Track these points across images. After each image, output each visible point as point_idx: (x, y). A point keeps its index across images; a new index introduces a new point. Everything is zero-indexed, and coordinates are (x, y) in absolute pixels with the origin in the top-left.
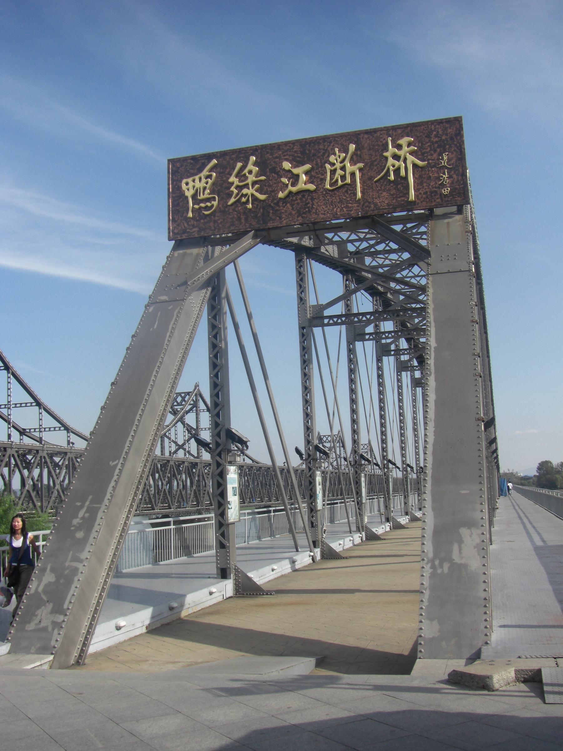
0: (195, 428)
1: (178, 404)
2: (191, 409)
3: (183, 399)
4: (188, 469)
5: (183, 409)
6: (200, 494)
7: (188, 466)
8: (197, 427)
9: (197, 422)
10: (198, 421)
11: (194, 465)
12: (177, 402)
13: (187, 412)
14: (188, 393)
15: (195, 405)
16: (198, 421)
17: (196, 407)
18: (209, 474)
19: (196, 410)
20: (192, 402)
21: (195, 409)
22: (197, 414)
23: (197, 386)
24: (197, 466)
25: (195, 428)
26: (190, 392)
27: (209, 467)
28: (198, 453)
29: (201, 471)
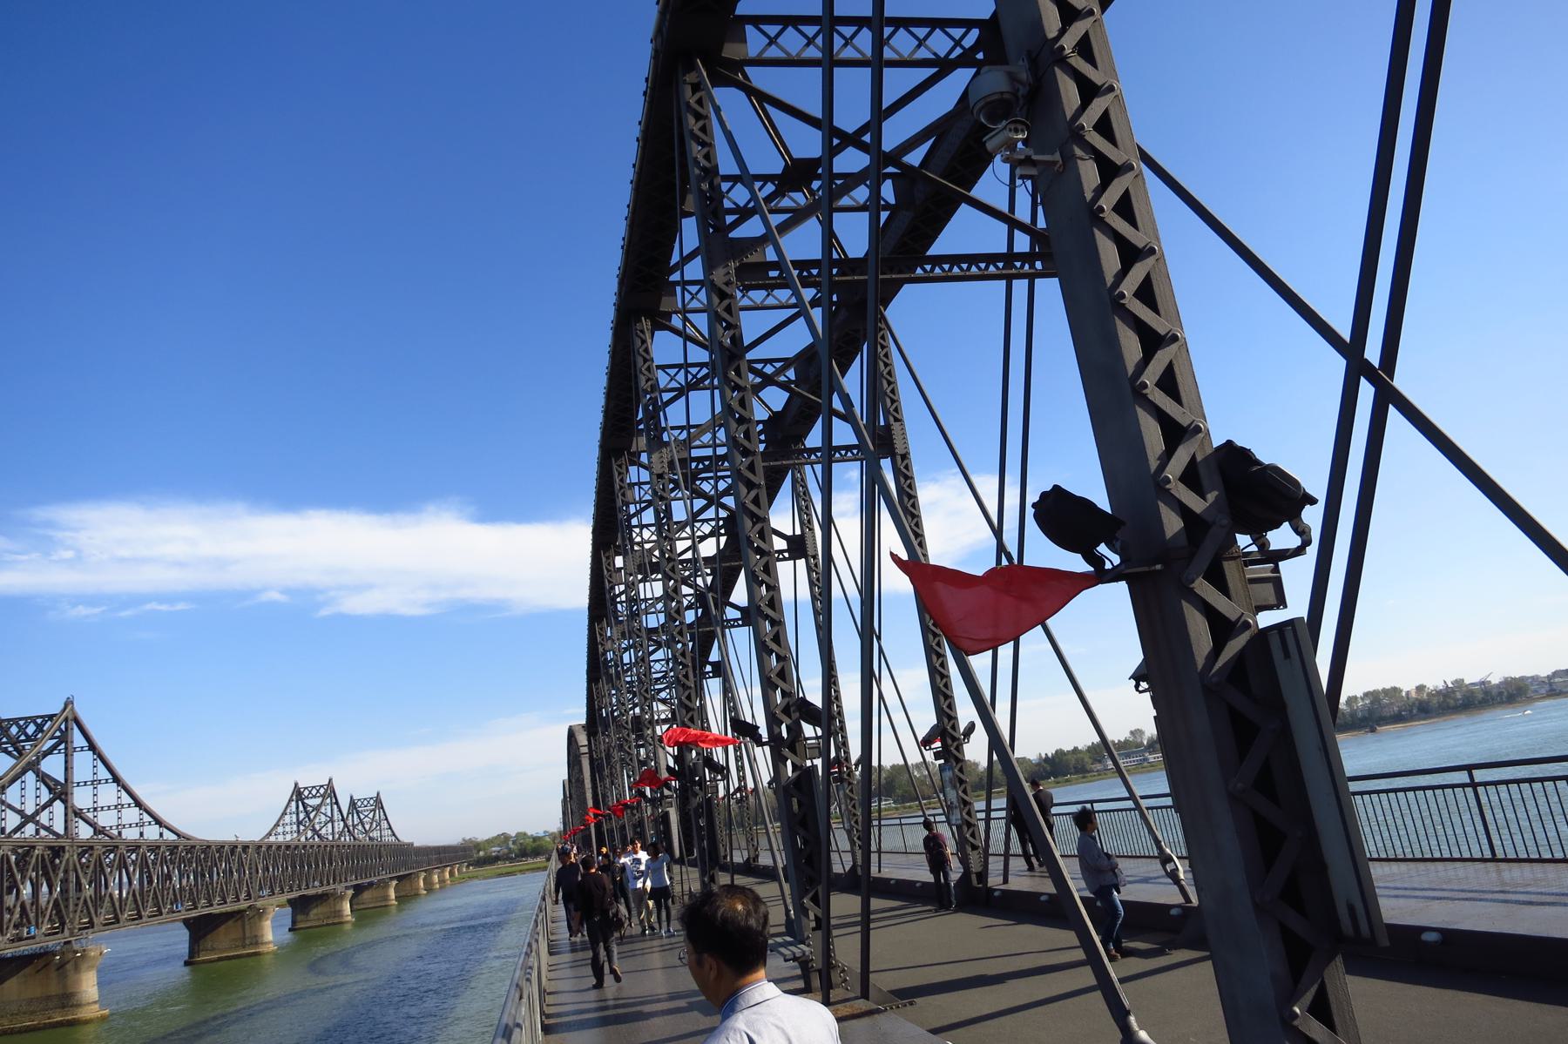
0: (63, 781)
1: (28, 739)
2: (54, 747)
3: (39, 728)
4: (43, 859)
5: (36, 746)
6: (67, 907)
7: (42, 855)
8: (66, 780)
9: (66, 769)
10: (68, 768)
11: (57, 851)
12: (26, 735)
13: (50, 752)
14: (51, 717)
15: (64, 738)
16: (68, 768)
17: (66, 742)
18: (88, 867)
19: (66, 748)
20: (58, 734)
21: (62, 746)
22: (66, 755)
23: (69, 703)
24: (64, 852)
25: (63, 781)
26: (55, 715)
27: (90, 852)
28: (66, 828)
29: (71, 862)
